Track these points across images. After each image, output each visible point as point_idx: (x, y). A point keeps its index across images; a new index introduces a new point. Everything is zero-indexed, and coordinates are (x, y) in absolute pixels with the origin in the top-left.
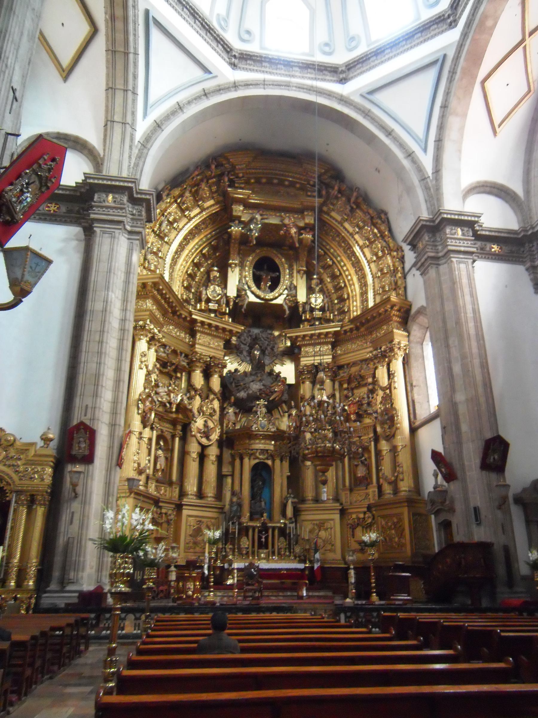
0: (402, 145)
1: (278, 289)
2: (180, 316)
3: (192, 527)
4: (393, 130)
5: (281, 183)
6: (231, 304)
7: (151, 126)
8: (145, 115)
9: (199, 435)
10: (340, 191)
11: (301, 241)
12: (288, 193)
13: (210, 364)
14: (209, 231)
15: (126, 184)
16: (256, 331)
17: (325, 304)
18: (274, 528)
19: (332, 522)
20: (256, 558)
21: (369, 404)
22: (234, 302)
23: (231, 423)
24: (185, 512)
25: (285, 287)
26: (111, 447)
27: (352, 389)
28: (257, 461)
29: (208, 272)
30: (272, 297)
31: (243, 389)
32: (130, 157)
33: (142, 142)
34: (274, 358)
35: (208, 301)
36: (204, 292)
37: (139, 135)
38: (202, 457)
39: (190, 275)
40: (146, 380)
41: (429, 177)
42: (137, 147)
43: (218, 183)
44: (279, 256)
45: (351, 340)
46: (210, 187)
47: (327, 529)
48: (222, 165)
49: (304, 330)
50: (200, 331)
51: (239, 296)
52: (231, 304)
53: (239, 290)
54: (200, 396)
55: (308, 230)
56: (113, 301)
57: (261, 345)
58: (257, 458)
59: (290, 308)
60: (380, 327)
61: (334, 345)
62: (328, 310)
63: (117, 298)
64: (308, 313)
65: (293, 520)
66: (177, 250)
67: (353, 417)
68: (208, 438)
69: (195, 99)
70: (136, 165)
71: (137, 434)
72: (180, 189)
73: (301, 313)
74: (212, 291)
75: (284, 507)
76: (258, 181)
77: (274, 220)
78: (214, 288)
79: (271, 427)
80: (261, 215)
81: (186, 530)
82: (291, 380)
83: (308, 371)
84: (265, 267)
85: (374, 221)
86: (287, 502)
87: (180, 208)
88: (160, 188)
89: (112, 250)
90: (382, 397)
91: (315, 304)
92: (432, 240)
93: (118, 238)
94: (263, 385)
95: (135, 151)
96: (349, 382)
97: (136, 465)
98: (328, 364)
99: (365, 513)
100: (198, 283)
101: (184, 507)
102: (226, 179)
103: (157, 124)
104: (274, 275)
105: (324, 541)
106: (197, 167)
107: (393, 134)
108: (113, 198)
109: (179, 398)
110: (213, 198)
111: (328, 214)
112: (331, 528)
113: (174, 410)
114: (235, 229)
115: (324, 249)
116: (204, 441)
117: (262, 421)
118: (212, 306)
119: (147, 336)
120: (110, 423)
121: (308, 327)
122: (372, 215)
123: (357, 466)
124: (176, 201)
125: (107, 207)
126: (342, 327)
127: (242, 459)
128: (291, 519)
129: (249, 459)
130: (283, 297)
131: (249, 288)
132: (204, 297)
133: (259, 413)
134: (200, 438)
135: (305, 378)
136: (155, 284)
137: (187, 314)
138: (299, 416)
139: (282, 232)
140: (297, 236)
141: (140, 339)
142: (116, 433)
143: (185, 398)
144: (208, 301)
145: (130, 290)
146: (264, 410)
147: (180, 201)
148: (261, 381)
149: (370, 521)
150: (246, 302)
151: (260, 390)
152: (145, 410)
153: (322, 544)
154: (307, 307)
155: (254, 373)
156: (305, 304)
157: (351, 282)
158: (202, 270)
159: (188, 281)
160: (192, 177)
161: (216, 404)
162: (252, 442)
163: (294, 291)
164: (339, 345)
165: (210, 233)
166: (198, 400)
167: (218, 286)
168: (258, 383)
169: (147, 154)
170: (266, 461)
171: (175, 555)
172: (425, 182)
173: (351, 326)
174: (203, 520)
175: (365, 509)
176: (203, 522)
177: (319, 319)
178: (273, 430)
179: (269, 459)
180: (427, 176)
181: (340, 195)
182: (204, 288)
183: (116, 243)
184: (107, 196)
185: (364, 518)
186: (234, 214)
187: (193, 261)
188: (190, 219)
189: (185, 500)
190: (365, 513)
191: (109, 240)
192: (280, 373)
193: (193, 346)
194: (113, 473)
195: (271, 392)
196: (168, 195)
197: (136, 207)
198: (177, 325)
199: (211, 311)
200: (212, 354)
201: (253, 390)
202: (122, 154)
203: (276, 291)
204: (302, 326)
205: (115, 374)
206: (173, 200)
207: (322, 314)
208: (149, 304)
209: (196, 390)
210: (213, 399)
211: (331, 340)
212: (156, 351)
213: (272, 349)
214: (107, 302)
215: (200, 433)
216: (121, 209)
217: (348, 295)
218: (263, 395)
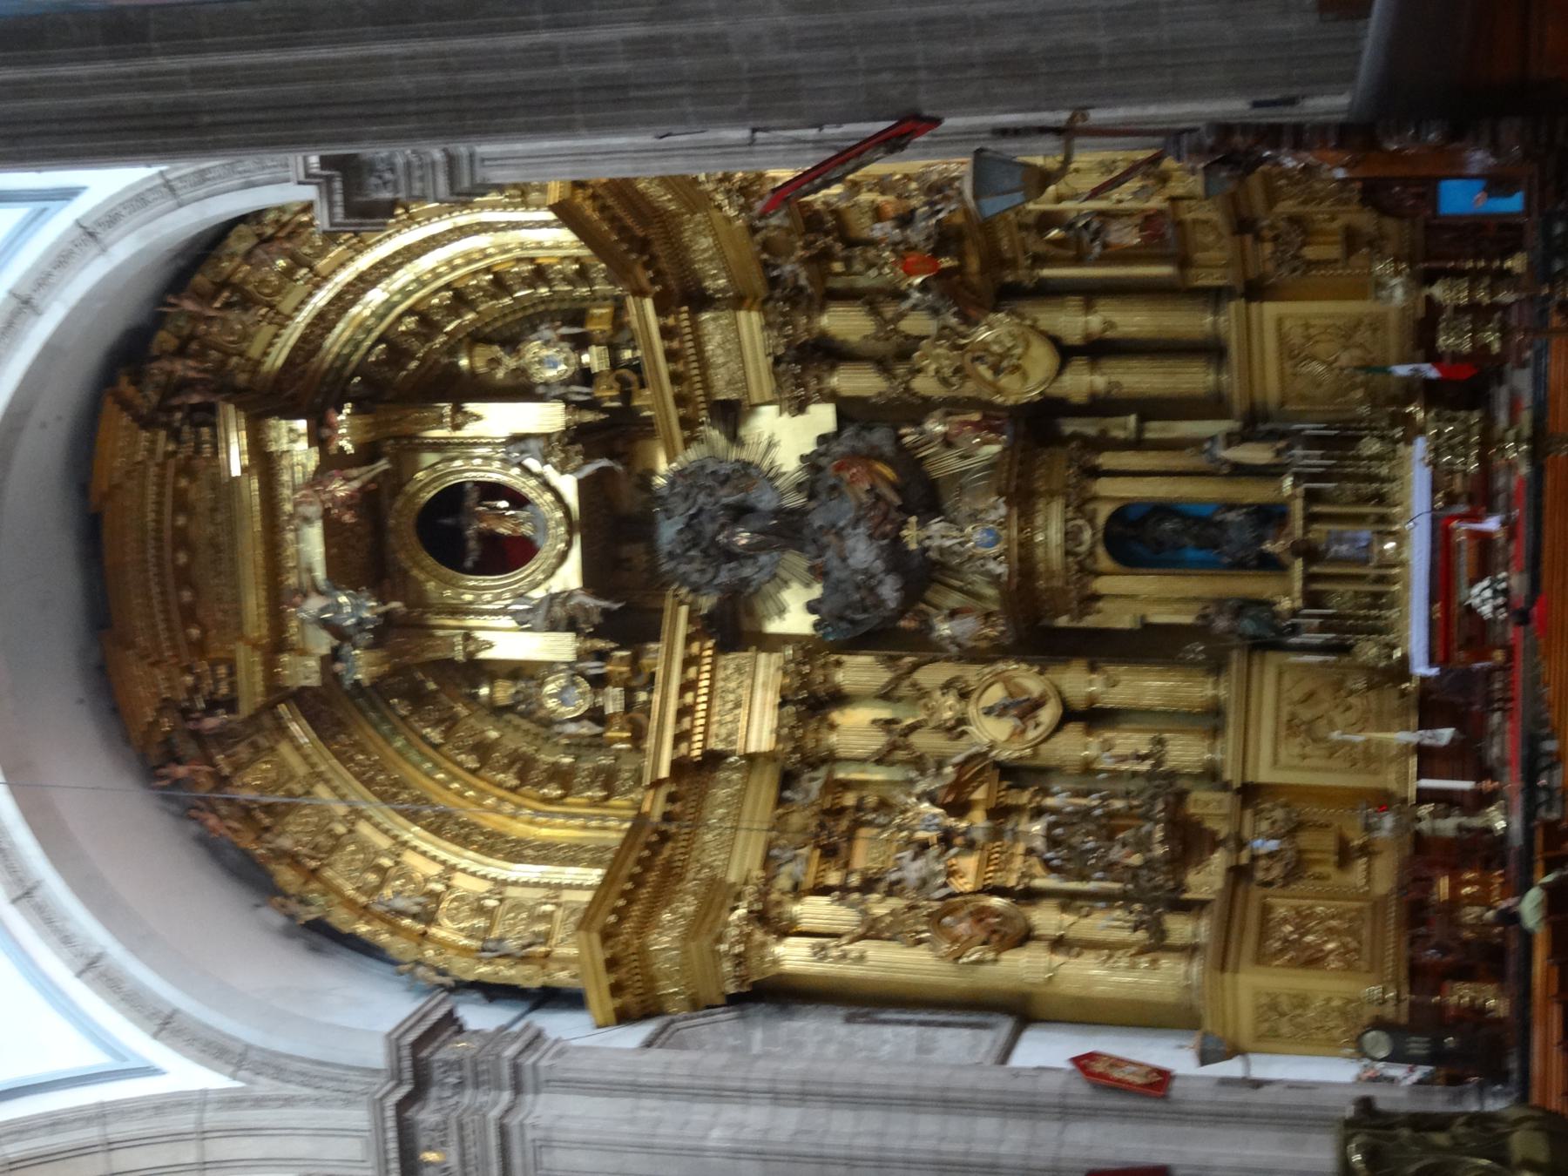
0: (61, 260)
1: (525, 491)
2: (667, 817)
3: (1308, 750)
4: (12, 294)
5: (182, 540)
6: (600, 644)
7: (169, 1045)
8: (149, 1071)
9: (1032, 734)
10: (181, 352)
11: (367, 453)
12: (214, 510)
13: (802, 702)
14: (371, 732)
15: (391, 1123)
16: (668, 532)
17: (563, 338)
18: (1311, 518)
19: (1287, 324)
20: (1396, 571)
21: (905, 220)
22: (591, 636)
23: (987, 631)
24: (1264, 774)
25: (516, 471)
26: (1123, 1115)
27: (851, 243)
28: (1101, 551)
29: (497, 711)
30: (559, 514)
31: (872, 590)
32: (288, 1101)
33: (231, 1069)
34: (753, 472)
35: (596, 715)
36: (572, 728)
37: (214, 1080)
38: (1094, 717)
39: (523, 777)
40: (889, 939)
41: (161, 173)
42: (251, 1082)
43: (224, 738)
44: (410, 488)
45: (680, 253)
46: (238, 767)
47: (1309, 338)
48: (167, 740)
49: (657, 401)
50: (705, 740)
51: (571, 625)
52: (600, 644)
53: (553, 627)
54: (913, 728)
55: (326, 432)
56: (729, 1133)
57: (716, 526)
58: (1091, 553)
59: (588, 457)
60: (642, 196)
61: (700, 300)
62: (581, 323)
63: (715, 1115)
64: (598, 394)
65: (1281, 444)
66: (453, 840)
67: (946, 262)
68: (1038, 704)
69: (49, 921)
70: (306, 1079)
71: (1058, 959)
72: (273, 867)
73: (602, 416)
74: (564, 703)
75: (1240, 471)
76: (189, 615)
77: (312, 544)
78: (551, 696)
79: (993, 516)
80: (305, 596)
81: (1316, 769)
82: (823, 417)
83: (798, 386)
84: (448, 521)
85: (269, 231)
86: (1226, 462)
87: (332, 850)
88: (278, 920)
89: (585, 1145)
90: (883, 193)
91: (562, 367)
92: (388, 176)
93: (548, 1129)
94: (856, 523)
95: (265, 1086)
96: (826, 256)
97: (1144, 962)
98: (768, 325)
99: (1259, 238)
100: (539, 742)
101: (1250, 779)
102: (210, 723)
103: (161, 1030)
104: (475, 495)
105: (1345, 348)
106: (194, 819)
107: (25, 291)
108: (429, 1149)
109: (925, 806)
110: (272, 749)
111: (259, 363)
112: (1307, 326)
113: (963, 825)
114: (362, 666)
115: (368, 343)
116: (1048, 715)
117: (975, 535)
118: (613, 701)
119: (763, 945)
120: (1059, 1120)
121: (647, 392)
122: (254, 241)
123: (1105, 245)
124: (314, 873)
125: (463, 1163)
126: (640, 293)
127: (1097, 597)
128: (1279, 453)
129: (1099, 574)
130: (551, 473)
131: (537, 585)
132: (587, 729)
133: (948, 543)
134: (1041, 729)
135: (819, 391)
136: (607, 936)
137: (663, 792)
138: (949, 414)
139: (348, 518)
140: (354, 472)
141: (776, 962)
142: (1084, 1102)
143: (922, 786)
144: (596, 715)
145: (685, 1081)
146: (936, 526)
147: (313, 858)
148: (839, 534)
149: (1282, 224)
150: (590, 602)
151: (871, 536)
152: (983, 936)
153: (1357, 353)
154: (579, 392)
155: (811, 548)
156: (571, 405)
157: (476, 256)
158: (493, 734)
159: (540, 785)
160: (230, 835)
161: (932, 676)
162: (1041, 567)
163: (533, 445)
164: (699, 282)
165: (375, 727)
166: (924, 741)
167: (542, 684)
168: (850, 543)
169: (262, 1050)
170: (1101, 519)
171: (1388, 821)
172: (178, 184)
173: (638, 270)
174: (1285, 717)
175: (1249, 238)
176: (1293, 716)
177: (613, 349)
178: (1003, 510)
179: (1095, 512)
180: (159, 181)
181: (194, 346)
182: (557, 728)
183: (563, 1136)
184: (429, 1164)
185: (1275, 239)
186: (314, 681)
187: (473, 772)
188: (357, 814)
189: (1228, 776)
190: (1259, 238)
191: (558, 1153)
192: (803, 458)
193: (751, 758)
194: (1188, 1107)
195: (874, 506)
196: (303, 902)
197: (437, 1075)
198: (698, 823)
199: (629, 705)
200: (772, 697)
201: (871, 557)
202: (293, 1132)
203: (532, 495)
204: (647, 413)
205: (926, 1113)
206: (314, 885)
207: (598, 345)
208: (664, 941)
209: (893, 747)
210: (914, 685)
211: (685, 316)
212: (798, 892)
213: (726, 480)
214: (738, 1151)
215: (1023, 731)
216: (461, 1127)
217: (519, 260)
218: (888, 527)
